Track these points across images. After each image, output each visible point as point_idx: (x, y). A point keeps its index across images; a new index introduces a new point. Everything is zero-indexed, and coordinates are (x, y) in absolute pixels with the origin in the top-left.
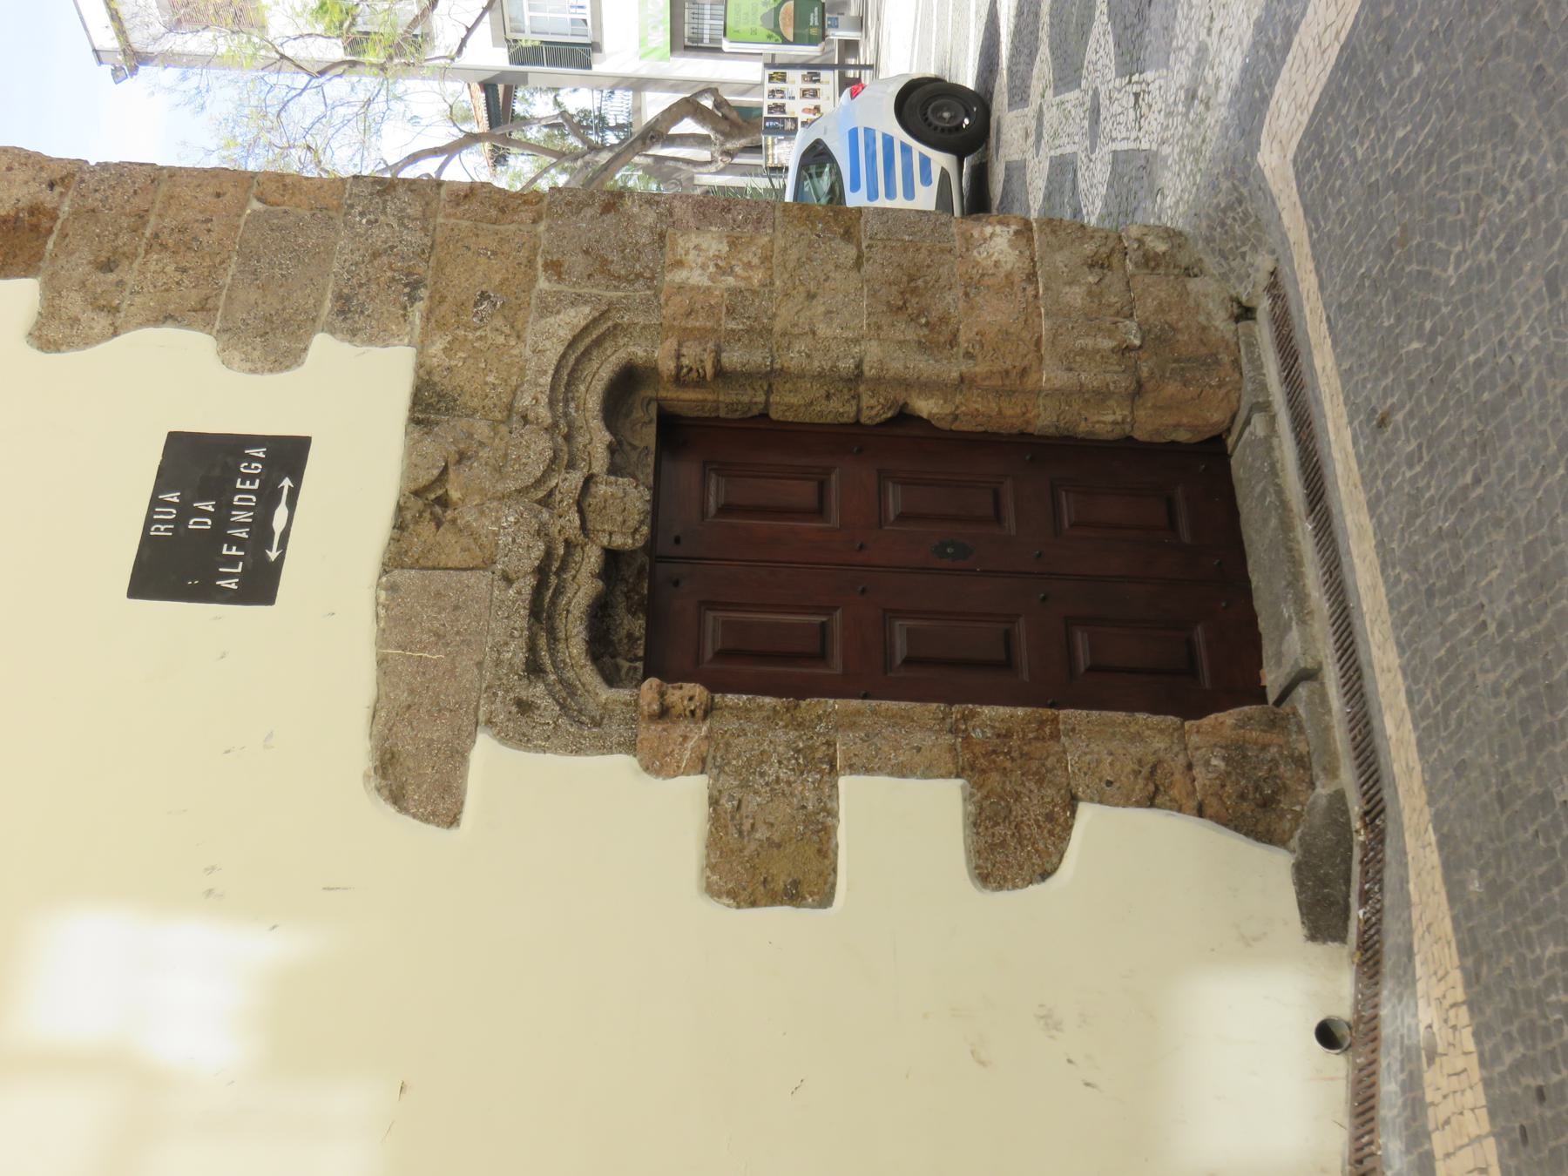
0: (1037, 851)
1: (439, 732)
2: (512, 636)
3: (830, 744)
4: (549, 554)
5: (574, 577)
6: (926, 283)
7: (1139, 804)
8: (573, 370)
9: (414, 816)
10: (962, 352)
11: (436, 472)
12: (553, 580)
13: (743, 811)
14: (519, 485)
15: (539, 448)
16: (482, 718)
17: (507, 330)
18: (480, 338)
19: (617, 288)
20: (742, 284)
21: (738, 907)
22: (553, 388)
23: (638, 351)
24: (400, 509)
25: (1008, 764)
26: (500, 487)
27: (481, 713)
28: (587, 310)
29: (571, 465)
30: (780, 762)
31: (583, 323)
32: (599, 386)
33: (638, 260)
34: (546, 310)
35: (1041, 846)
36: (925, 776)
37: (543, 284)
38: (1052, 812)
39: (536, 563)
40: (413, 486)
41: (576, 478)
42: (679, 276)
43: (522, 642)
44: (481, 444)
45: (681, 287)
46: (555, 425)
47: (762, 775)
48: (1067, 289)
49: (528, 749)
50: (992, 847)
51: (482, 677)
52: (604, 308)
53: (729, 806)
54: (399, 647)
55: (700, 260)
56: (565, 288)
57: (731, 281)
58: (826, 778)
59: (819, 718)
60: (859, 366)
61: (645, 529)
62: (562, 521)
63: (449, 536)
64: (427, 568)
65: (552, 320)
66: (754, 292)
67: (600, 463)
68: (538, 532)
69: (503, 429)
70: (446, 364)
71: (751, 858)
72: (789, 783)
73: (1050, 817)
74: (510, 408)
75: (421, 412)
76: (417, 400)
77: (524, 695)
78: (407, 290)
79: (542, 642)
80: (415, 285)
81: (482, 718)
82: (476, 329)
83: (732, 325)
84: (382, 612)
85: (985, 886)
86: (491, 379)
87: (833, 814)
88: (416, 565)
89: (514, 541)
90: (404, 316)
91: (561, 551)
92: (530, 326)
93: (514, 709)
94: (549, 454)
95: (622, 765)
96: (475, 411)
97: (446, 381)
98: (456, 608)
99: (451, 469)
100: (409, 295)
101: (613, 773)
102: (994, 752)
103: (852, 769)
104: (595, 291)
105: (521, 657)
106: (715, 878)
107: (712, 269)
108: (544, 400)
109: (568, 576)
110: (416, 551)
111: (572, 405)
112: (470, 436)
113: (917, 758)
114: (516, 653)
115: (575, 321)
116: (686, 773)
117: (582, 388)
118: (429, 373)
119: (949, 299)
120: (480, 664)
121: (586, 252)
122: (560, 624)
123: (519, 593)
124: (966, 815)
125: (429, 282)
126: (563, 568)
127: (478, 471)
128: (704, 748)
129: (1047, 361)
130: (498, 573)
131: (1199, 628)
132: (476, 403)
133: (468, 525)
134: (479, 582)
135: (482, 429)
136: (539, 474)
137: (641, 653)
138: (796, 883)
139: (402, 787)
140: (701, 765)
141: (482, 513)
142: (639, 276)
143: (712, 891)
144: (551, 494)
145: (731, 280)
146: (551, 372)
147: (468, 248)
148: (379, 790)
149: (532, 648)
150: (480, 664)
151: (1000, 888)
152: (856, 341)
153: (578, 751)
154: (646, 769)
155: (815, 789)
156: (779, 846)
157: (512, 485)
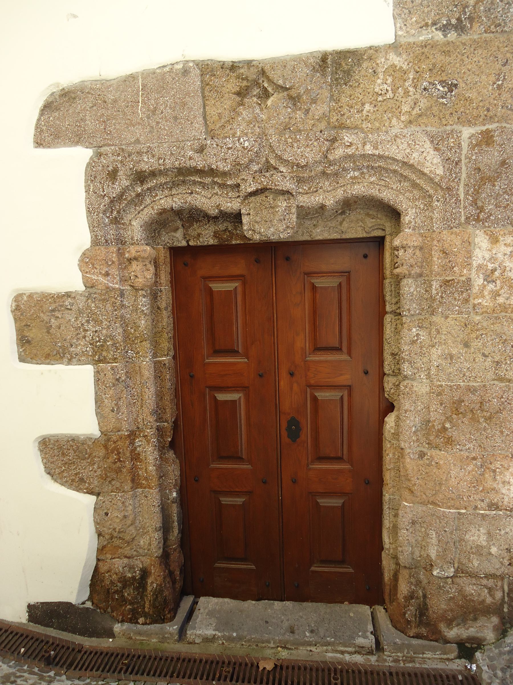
0: (63, 472)
1: (90, 124)
2: (159, 158)
3: (115, 360)
4: (225, 174)
5: (217, 194)
6: (485, 429)
7: (96, 528)
8: (386, 170)
9: (39, 120)
10: (425, 450)
11: (280, 82)
12: (208, 180)
13: (67, 311)
14: (275, 144)
15: (309, 153)
16: (102, 150)
17: (416, 111)
18: (406, 93)
19: (467, 194)
20: (475, 290)
21: (12, 311)
22: (364, 156)
23: (409, 217)
24: (249, 63)
25: (110, 460)
26: (271, 131)
27: (108, 148)
28: (440, 171)
29: (300, 181)
30: (96, 331)
31: (426, 171)
32: (374, 192)
33: (497, 206)
34: (437, 142)
35: (65, 474)
36: (97, 414)
37: (467, 132)
38: (85, 482)
39: (214, 166)
40: (267, 68)
41: (288, 185)
42: (481, 240)
43: (156, 166)
44: (307, 111)
45: (468, 244)
46: (331, 163)
47: (88, 322)
48: (483, 530)
49: (86, 181)
50: (60, 448)
51: (128, 145)
52: (444, 185)
53: (67, 303)
54: (144, 86)
55: (500, 256)
56: (464, 152)
57: (479, 281)
58: (90, 358)
59: (138, 353)
60: (406, 377)
61: (257, 237)
62: (250, 179)
63: (229, 103)
64: (203, 93)
65: (428, 145)
66: (467, 301)
67: (304, 200)
68: (239, 164)
69: (322, 125)
70: (380, 70)
71: (39, 317)
72: (84, 337)
73: (82, 480)
74: (342, 126)
75: (334, 61)
76: (343, 55)
77: (120, 173)
78: (454, 21)
79: (162, 180)
80: (459, 27)
81: (102, 150)
82: (415, 87)
83: (435, 285)
84: (167, 69)
85: (40, 443)
86: (367, 107)
87: (70, 362)
88: (205, 84)
89: (229, 149)
90: (427, 25)
91: (229, 183)
92: (417, 129)
93: (110, 168)
94: (303, 162)
95: (84, 239)
96: (337, 101)
97: (363, 73)
98: (176, 118)
99: (286, 93)
100: (449, 24)
101: (78, 234)
102: (119, 453)
103: (97, 373)
104: (464, 176)
105: (144, 167)
106: (25, 298)
107: (490, 266)
108: (350, 151)
109: (216, 189)
110: (216, 82)
111: (357, 174)
112: (314, 101)
113: (107, 410)
114: (147, 163)
115: (428, 164)
116: (84, 277)
117: (373, 179)
118: (370, 58)
119: (471, 446)
120: (138, 141)
121: (503, 163)
122: (182, 189)
123: (190, 158)
124: (78, 437)
125: (464, 38)
126: (223, 186)
127: (285, 113)
128: (100, 287)
129: (420, 509)
130: (204, 143)
131: (253, 567)
132: (344, 100)
133: (239, 114)
134: (197, 130)
135: (319, 109)
136: (285, 157)
137: (191, 243)
138: (28, 342)
139: (57, 109)
140: (89, 285)
141: (250, 122)
142: (481, 209)
143: (18, 298)
144: (275, 168)
145: (480, 281)
146: (377, 152)
147: (504, 65)
148: (52, 94)
149: (153, 174)
150: (138, 141)
151: (41, 451)
152: (428, 376)
153: (89, 212)
154: (84, 254)
155: (83, 352)
156: (48, 332)
157: (274, 139)
